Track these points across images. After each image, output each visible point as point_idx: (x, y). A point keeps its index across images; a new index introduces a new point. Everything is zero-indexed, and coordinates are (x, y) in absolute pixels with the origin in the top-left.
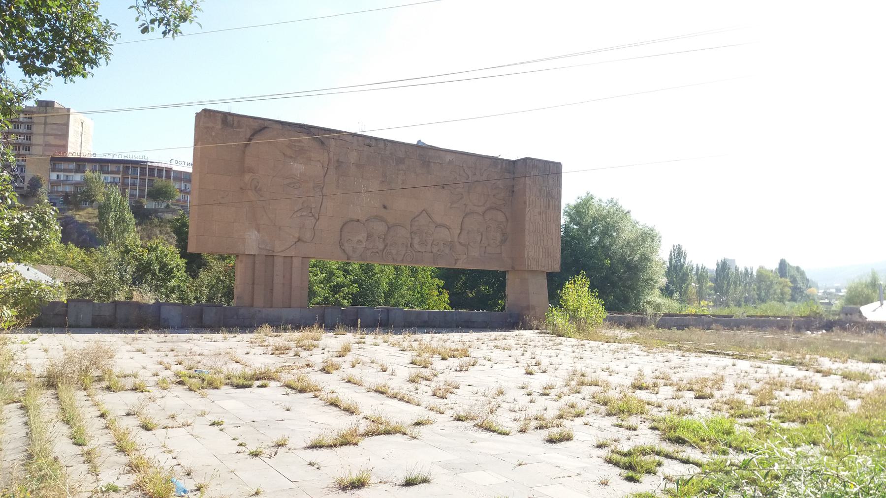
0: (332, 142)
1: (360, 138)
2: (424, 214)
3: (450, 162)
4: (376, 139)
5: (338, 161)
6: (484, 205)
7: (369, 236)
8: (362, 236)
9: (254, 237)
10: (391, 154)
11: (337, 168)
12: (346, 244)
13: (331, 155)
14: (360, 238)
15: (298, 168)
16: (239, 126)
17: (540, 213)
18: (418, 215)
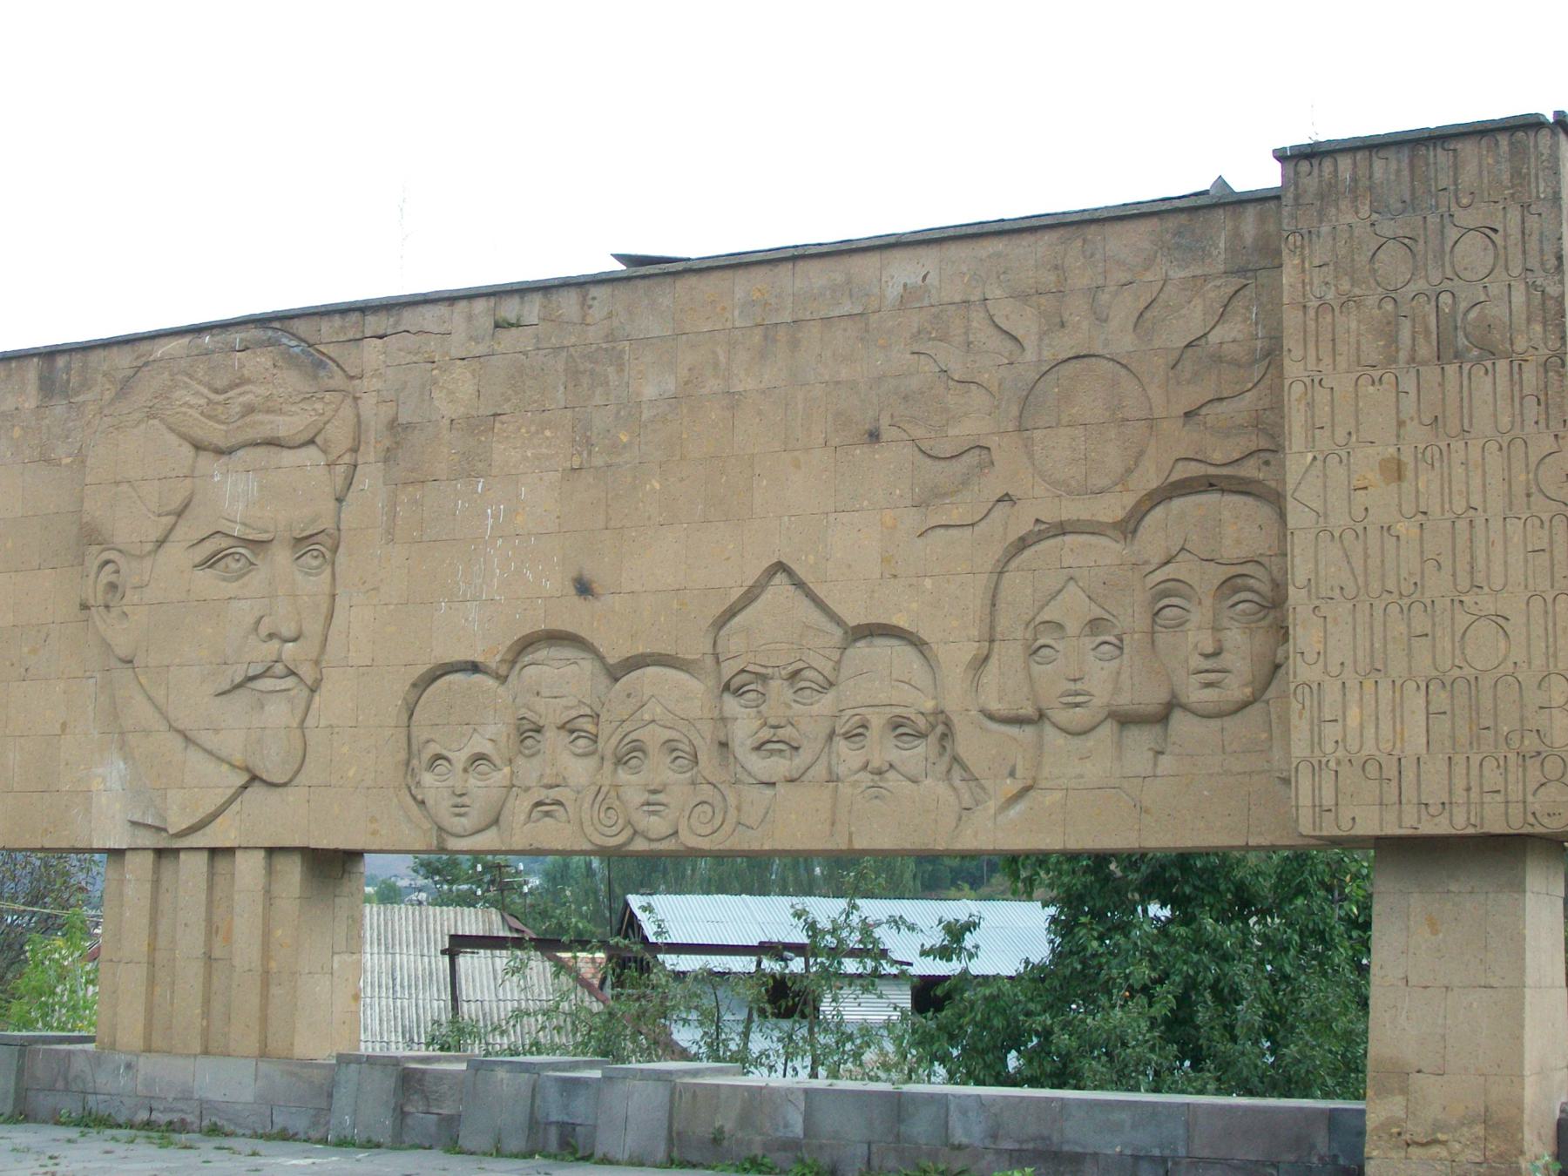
0: (372, 352)
1: (480, 305)
2: (780, 586)
3: (908, 297)
4: (546, 288)
5: (393, 425)
6: (1123, 480)
7: (528, 731)
8: (491, 735)
9: (117, 786)
10: (610, 337)
11: (388, 457)
12: (428, 778)
13: (368, 404)
14: (480, 744)
15: (236, 494)
16: (85, 385)
17: (1395, 471)
18: (750, 596)
